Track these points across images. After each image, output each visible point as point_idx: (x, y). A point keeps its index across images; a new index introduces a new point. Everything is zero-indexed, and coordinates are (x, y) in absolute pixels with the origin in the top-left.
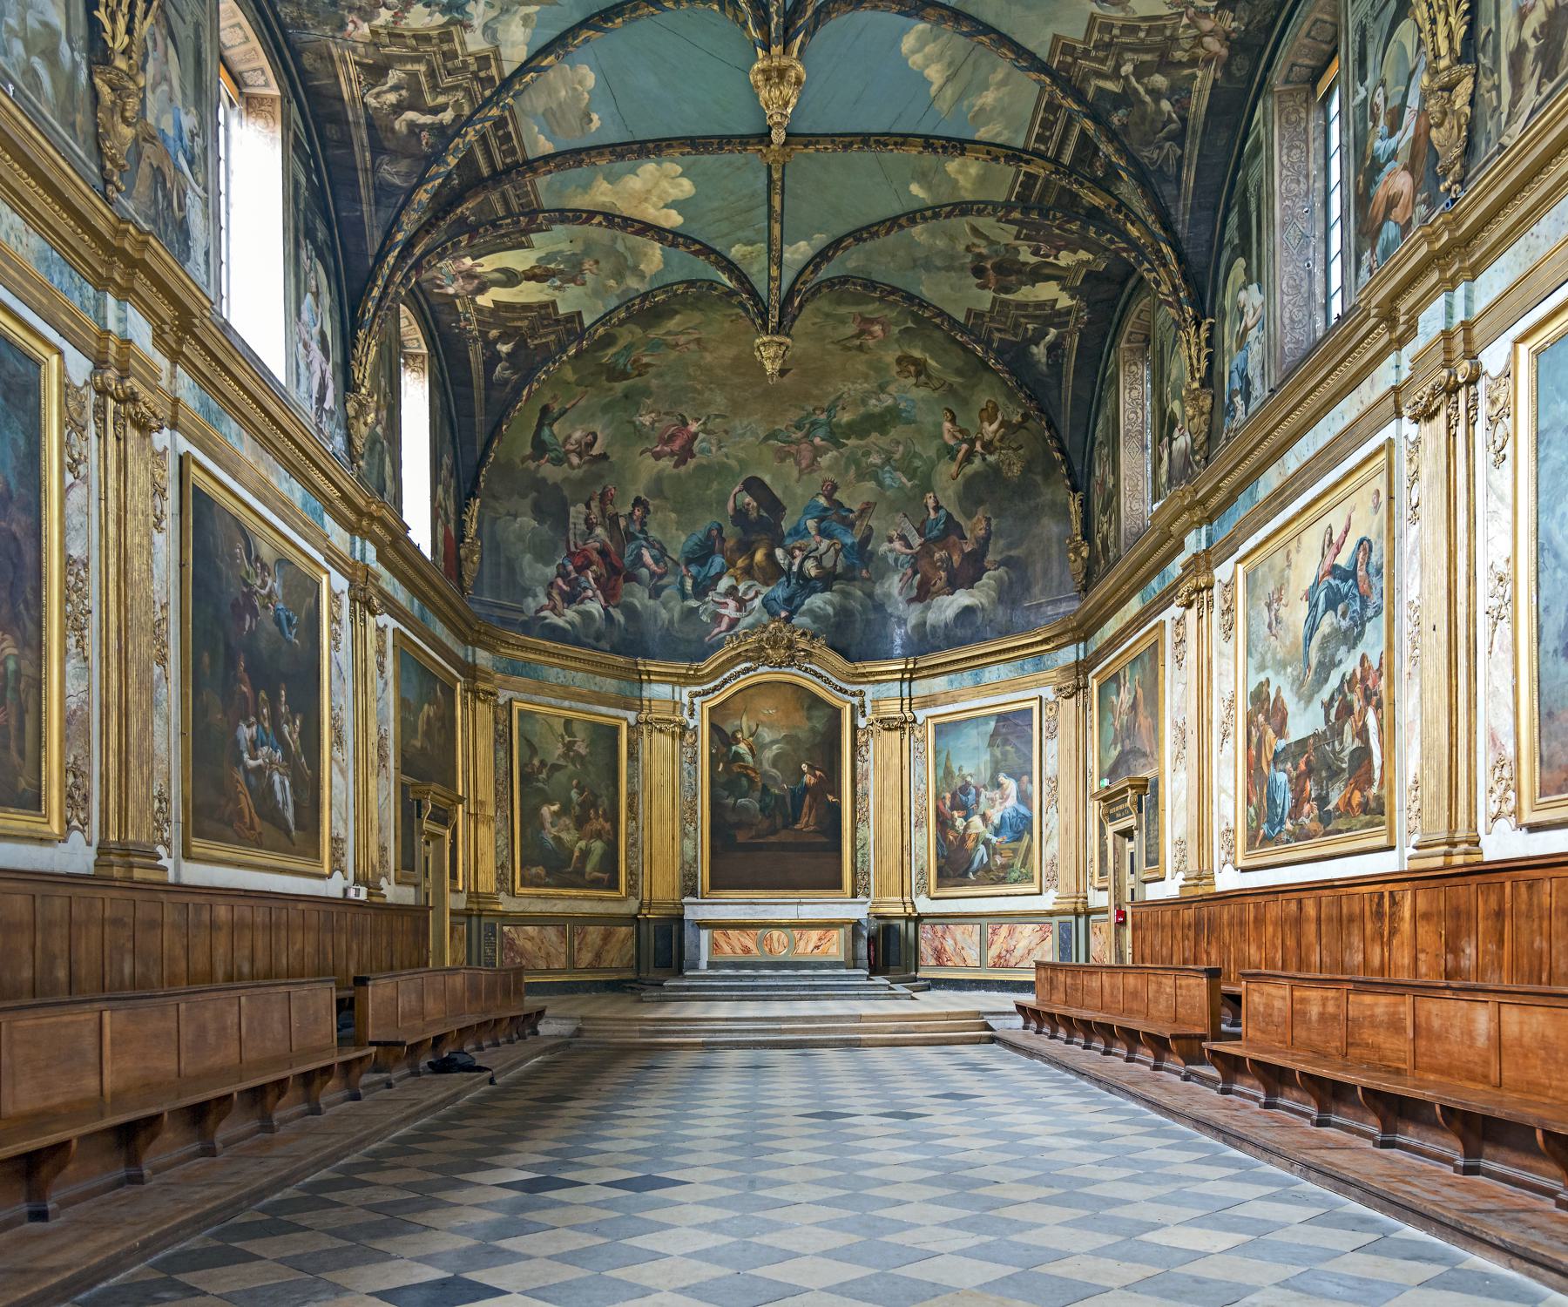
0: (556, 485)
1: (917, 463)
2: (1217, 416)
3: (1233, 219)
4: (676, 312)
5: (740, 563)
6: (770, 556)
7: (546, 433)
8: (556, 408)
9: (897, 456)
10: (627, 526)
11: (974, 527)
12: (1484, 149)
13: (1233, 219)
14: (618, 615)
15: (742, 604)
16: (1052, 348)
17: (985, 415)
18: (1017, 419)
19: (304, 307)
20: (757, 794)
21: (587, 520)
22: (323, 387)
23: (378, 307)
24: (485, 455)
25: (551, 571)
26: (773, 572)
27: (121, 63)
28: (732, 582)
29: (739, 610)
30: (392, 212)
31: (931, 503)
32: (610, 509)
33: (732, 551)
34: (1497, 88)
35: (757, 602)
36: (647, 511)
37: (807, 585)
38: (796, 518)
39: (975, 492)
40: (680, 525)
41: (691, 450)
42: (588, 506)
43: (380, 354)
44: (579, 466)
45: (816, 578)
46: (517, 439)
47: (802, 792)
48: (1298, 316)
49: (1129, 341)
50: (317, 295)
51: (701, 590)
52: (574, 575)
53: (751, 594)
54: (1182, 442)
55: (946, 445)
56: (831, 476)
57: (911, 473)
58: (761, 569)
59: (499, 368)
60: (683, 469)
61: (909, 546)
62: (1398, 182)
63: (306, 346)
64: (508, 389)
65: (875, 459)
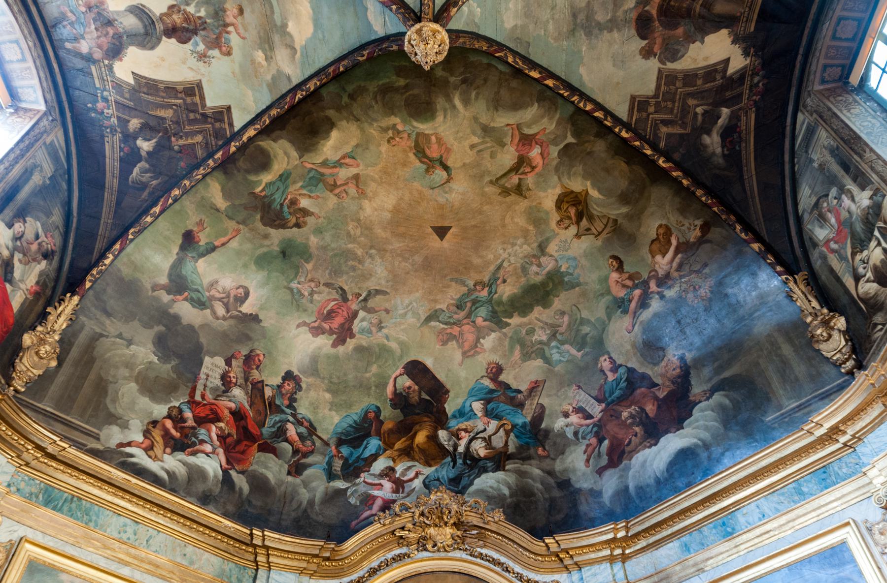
0: (191, 327)
1: (586, 329)
4: (331, 125)
5: (398, 445)
6: (433, 438)
8: (203, 239)
9: (562, 329)
10: (274, 397)
14: (241, 481)
15: (399, 485)
16: (730, 133)
17: (656, 246)
18: (694, 234)
21: (224, 377)
25: (160, 410)
28: (391, 464)
29: (396, 491)
31: (606, 364)
32: (256, 375)
33: (391, 431)
35: (417, 483)
36: (300, 388)
38: (460, 401)
40: (334, 406)
41: (350, 329)
42: (228, 362)
44: (224, 318)
45: (486, 458)
49: (823, 81)
51: (352, 470)
52: (191, 423)
53: (411, 474)
55: (615, 299)
56: (496, 358)
57: (581, 344)
58: (422, 451)
59: (136, 170)
60: (341, 349)
64: (145, 194)
65: (541, 335)
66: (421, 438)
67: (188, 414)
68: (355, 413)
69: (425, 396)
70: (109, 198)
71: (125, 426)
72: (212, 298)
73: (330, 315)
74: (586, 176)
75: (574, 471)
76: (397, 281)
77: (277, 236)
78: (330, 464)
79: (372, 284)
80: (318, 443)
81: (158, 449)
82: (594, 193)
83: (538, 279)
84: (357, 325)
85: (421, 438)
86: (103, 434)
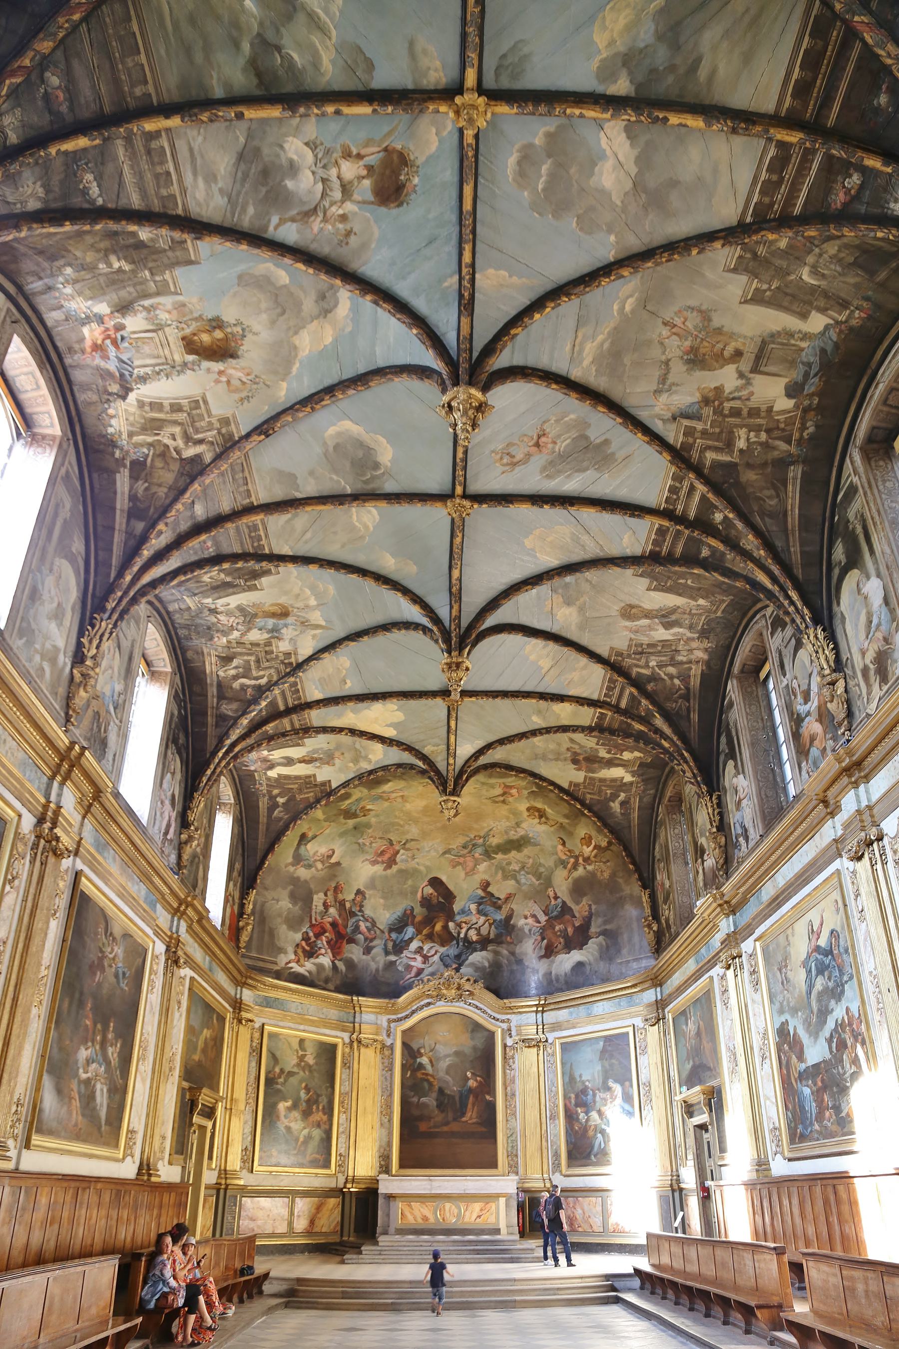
0: (306, 881)
1: (542, 870)
2: (729, 849)
3: (723, 739)
5: (425, 932)
6: (445, 927)
7: (303, 847)
8: (310, 834)
11: (580, 909)
12: (859, 716)
13: (723, 739)
14: (341, 966)
15: (426, 958)
16: (623, 804)
18: (604, 844)
19: (165, 781)
20: (434, 1095)
22: (168, 826)
23: (209, 780)
24: (262, 862)
25: (298, 937)
26: (446, 938)
27: (89, 663)
29: (424, 963)
30: (225, 730)
31: (552, 894)
32: (340, 897)
33: (420, 923)
34: (859, 685)
36: (365, 898)
37: (469, 946)
38: (463, 903)
39: (579, 889)
40: (386, 907)
42: (326, 895)
43: (205, 805)
45: (476, 942)
46: (284, 853)
47: (464, 1096)
48: (770, 793)
50: (173, 774)
51: (399, 948)
52: (313, 939)
53: (432, 952)
54: (710, 862)
57: (539, 876)
58: (439, 936)
60: (389, 872)
61: (539, 922)
62: (812, 726)
63: (162, 803)
65: (515, 867)
66: (438, 927)
67: (311, 934)
68: (399, 912)
69: (441, 900)
70: (262, 828)
71: (286, 953)
72: (316, 861)
73: (382, 853)
74: (544, 803)
75: (526, 954)
76: (425, 835)
77: (351, 823)
78: (385, 945)
79: (409, 837)
80: (378, 932)
81: (302, 961)
82: (549, 811)
83: (515, 838)
84: (399, 858)
85: (438, 927)
86: (278, 960)
